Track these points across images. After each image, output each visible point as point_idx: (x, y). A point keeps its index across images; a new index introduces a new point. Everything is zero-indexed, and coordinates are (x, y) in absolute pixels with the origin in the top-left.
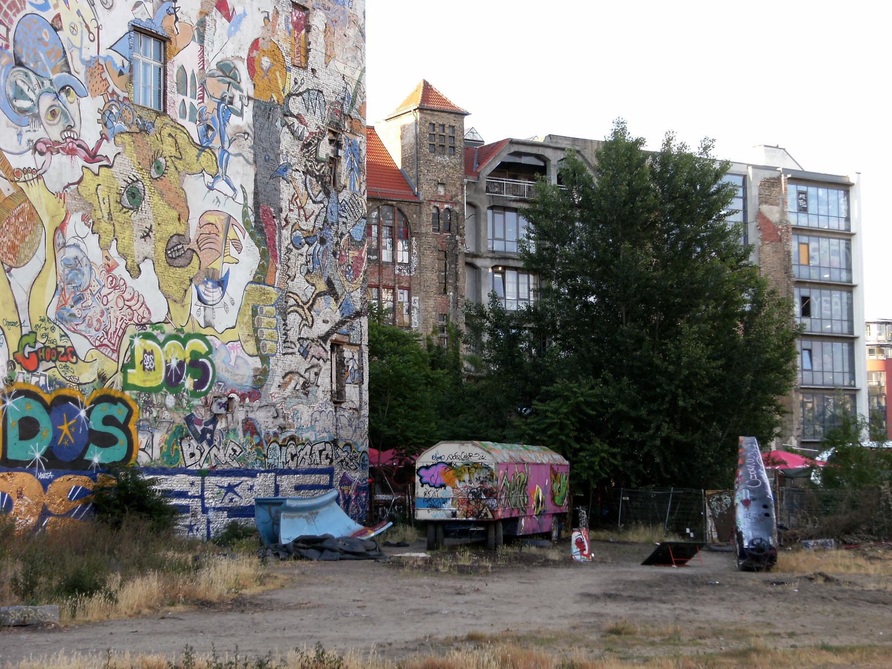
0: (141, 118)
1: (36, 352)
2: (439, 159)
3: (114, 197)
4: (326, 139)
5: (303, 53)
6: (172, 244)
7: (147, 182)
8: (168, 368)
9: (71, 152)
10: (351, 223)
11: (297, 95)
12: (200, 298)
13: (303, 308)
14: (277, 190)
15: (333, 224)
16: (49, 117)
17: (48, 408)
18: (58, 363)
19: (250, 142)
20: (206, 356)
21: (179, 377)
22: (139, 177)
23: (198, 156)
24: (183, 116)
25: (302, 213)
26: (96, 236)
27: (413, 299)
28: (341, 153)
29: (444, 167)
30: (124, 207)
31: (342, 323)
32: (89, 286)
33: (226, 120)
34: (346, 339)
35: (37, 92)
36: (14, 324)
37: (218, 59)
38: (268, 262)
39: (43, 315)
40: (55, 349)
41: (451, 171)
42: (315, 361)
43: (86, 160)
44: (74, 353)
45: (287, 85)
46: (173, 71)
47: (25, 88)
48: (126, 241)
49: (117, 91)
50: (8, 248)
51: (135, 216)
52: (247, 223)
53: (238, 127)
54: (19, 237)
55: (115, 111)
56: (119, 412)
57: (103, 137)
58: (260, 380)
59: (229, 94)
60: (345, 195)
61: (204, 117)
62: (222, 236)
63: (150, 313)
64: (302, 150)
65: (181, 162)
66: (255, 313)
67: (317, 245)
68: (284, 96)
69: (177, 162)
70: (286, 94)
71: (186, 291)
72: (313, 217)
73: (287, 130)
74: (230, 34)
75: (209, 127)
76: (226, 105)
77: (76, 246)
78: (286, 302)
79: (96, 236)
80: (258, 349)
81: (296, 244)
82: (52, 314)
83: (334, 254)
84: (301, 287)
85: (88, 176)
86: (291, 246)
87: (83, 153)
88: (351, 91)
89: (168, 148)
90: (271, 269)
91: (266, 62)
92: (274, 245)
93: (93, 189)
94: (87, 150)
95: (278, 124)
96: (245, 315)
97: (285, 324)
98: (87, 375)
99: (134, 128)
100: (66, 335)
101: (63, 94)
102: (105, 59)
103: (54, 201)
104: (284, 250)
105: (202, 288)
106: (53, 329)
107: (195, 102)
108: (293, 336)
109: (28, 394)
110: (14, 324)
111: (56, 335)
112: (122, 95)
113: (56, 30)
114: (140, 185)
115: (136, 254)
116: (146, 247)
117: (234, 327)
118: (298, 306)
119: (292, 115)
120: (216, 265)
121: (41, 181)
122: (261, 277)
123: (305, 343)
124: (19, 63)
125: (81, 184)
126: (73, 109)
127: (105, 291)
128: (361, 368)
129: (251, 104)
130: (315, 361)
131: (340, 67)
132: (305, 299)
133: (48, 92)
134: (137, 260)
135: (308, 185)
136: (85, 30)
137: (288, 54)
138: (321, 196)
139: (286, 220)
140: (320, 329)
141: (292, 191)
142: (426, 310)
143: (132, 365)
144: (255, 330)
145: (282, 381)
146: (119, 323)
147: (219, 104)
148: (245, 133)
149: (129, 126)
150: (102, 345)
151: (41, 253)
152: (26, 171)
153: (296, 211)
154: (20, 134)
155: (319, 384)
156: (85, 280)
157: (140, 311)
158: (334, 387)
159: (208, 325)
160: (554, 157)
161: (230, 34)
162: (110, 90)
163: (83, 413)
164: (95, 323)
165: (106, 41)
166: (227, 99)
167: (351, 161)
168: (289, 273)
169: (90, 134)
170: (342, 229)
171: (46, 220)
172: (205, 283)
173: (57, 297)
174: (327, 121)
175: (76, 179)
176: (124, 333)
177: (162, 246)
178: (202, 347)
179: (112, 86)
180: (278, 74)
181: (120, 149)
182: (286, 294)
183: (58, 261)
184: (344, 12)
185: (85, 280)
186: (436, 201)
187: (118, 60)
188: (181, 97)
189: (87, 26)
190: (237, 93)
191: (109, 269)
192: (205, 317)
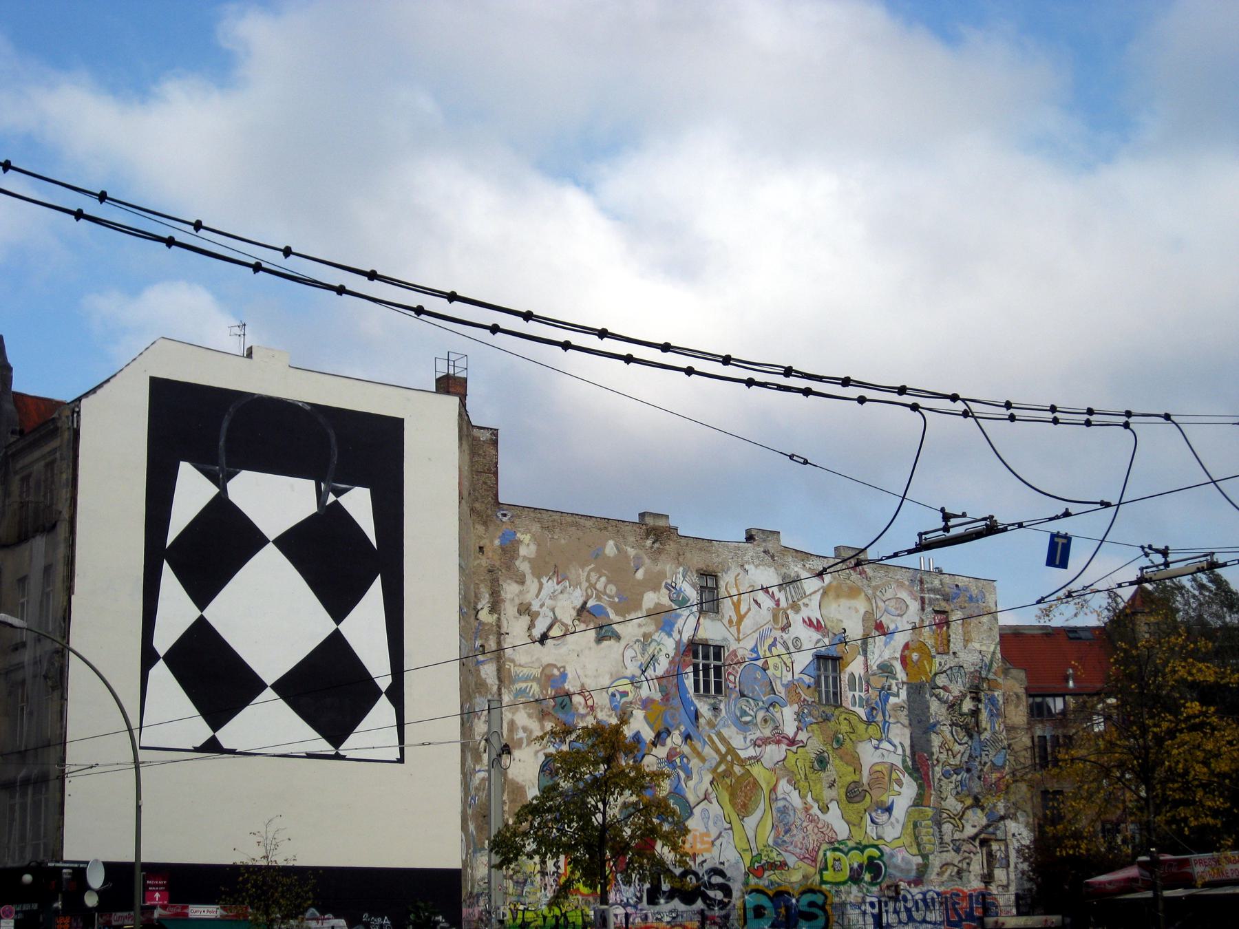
0: (824, 712)
1: (762, 866)
3: (808, 764)
4: (968, 698)
5: (945, 642)
6: (850, 788)
7: (831, 752)
8: (851, 869)
9: (778, 742)
10: (992, 753)
11: (942, 673)
12: (872, 821)
13: (954, 819)
14: (929, 741)
15: (977, 757)
16: (763, 723)
17: (771, 899)
18: (776, 871)
19: (905, 712)
20: (880, 858)
21: (859, 874)
22: (825, 749)
23: (867, 729)
24: (854, 704)
25: (950, 753)
26: (797, 791)
28: (980, 706)
30: (815, 770)
31: (988, 826)
33: (886, 700)
34: (993, 837)
35: (754, 710)
36: (747, 850)
37: (878, 662)
38: (924, 790)
39: (765, 843)
40: (774, 863)
42: (967, 855)
43: (788, 745)
44: (786, 864)
45: (933, 668)
46: (845, 677)
47: (747, 709)
48: (818, 791)
49: (807, 698)
50: (741, 806)
51: (823, 775)
52: (906, 768)
53: (896, 704)
54: (748, 798)
55: (806, 711)
56: (819, 899)
57: (799, 729)
58: (922, 871)
59: (888, 684)
60: (986, 735)
61: (870, 703)
62: (887, 778)
63: (836, 834)
64: (948, 710)
65: (854, 735)
66: (915, 826)
67: (964, 774)
68: (931, 676)
69: (851, 736)
70: (933, 674)
71: (862, 818)
72: (960, 755)
73: (935, 699)
74: (886, 644)
75: (873, 708)
76: (885, 693)
77: (784, 799)
78: (940, 816)
79: (797, 791)
80: (919, 850)
81: (946, 775)
82: (771, 842)
83: (979, 778)
84: (953, 804)
85: (790, 755)
86: (942, 778)
87: (786, 741)
88: (987, 661)
89: (845, 727)
90: (927, 795)
91: (915, 656)
92: (929, 779)
93: (793, 762)
94: (788, 739)
95: (927, 696)
96: (908, 829)
97: (941, 832)
98: (796, 877)
99: (820, 719)
100: (780, 854)
101: (771, 708)
102: (797, 680)
103: (768, 773)
104: (936, 780)
105: (874, 814)
106: (772, 851)
107: (862, 694)
108: (947, 838)
109: (758, 891)
110: (747, 850)
111: (774, 854)
112: (810, 700)
113: (765, 670)
114: (826, 754)
115: (825, 798)
116: (833, 793)
117: (899, 838)
118: (950, 817)
119: (939, 688)
120: (884, 798)
122: (919, 802)
123: (958, 843)
124: (743, 695)
125: (786, 760)
126: (778, 715)
127: (805, 824)
128: (1007, 857)
129: (905, 687)
130: (967, 855)
131: (977, 646)
132: (955, 812)
133: (761, 708)
134: (826, 802)
135: (954, 733)
136: (783, 665)
137: (933, 647)
138: (966, 739)
139: (937, 760)
140: (970, 831)
141: (941, 739)
143: (826, 868)
144: (916, 838)
145: (939, 870)
146: (815, 843)
148: (901, 707)
149: (817, 719)
150: (805, 858)
151: (762, 806)
152: (750, 758)
153: (945, 753)
154: (745, 738)
155: (971, 870)
156: (791, 819)
157: (830, 834)
158: (986, 871)
159: (880, 838)
161: (886, 644)
162: (802, 699)
163: (794, 901)
164: (799, 845)
167: (991, 710)
168: (942, 796)
169: (790, 729)
170: (985, 759)
171: (764, 786)
172: (876, 811)
173: (773, 831)
174: (968, 685)
175: (782, 758)
176: (819, 848)
177: (843, 791)
178: (876, 853)
179: (803, 696)
180: (925, 662)
181: (811, 734)
182: (939, 811)
183: (773, 809)
184: (978, 607)
185: (791, 819)
187: (807, 679)
188: (852, 693)
189: (785, 663)
190: (894, 682)
191: (807, 810)
192: (877, 833)
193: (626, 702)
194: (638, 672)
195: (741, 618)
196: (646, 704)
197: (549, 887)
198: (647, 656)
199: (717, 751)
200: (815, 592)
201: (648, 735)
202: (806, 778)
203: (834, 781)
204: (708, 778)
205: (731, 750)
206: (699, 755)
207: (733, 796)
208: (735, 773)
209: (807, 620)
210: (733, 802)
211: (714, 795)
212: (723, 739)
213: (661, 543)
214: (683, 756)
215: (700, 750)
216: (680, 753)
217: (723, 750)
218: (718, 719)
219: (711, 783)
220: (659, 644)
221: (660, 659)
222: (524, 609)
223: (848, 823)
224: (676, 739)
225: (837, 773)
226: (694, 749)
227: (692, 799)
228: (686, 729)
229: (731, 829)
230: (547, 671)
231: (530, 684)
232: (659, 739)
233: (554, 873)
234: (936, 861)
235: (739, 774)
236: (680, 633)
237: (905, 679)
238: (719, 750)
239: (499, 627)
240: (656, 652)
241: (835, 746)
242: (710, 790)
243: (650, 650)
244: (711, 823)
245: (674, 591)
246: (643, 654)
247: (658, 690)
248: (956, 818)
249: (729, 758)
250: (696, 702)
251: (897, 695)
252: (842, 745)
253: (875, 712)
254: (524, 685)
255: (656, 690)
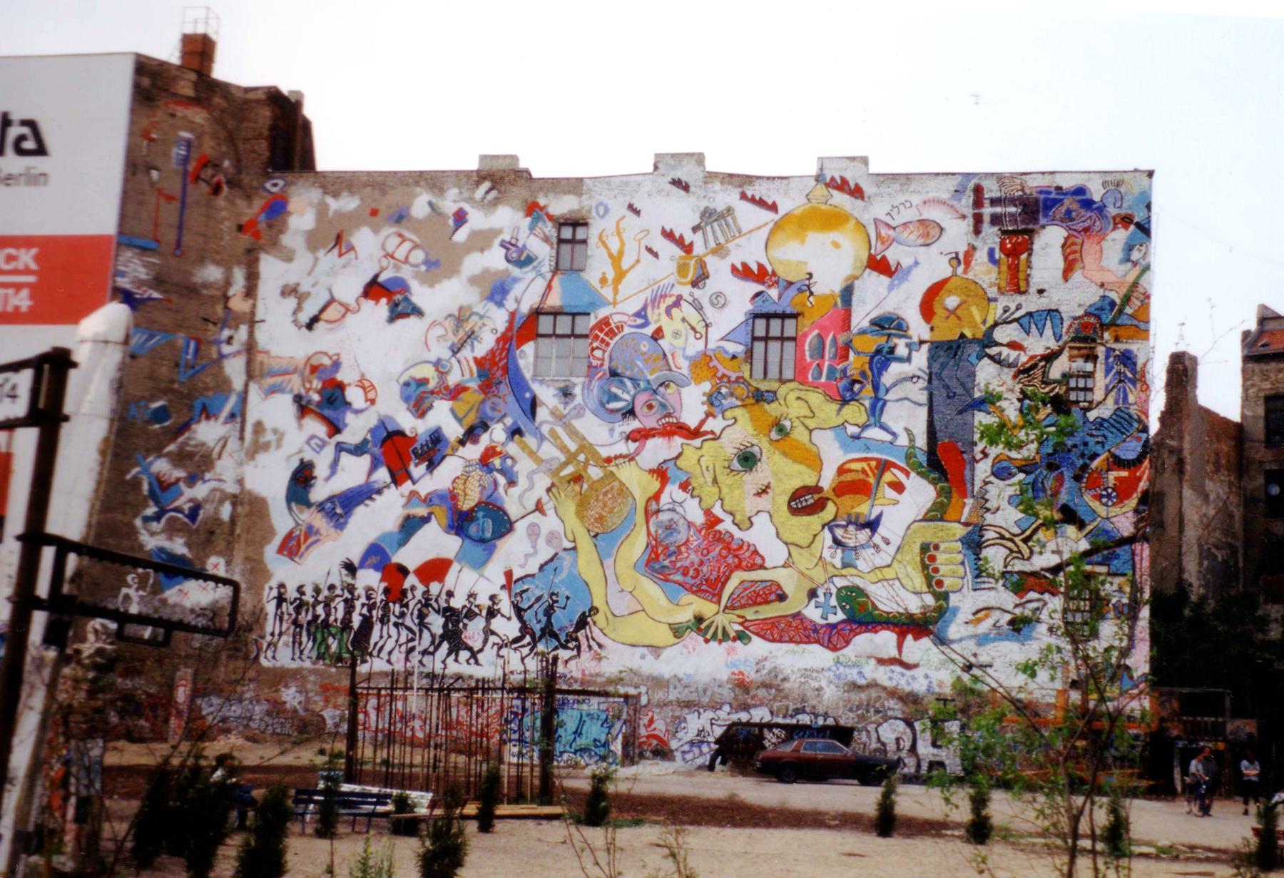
16: (645, 409)
19: (923, 383)
22: (755, 442)
26: (697, 500)
32: (688, 540)
35: (633, 392)
49: (729, 373)
51: (748, 477)
55: (724, 390)
57: (709, 415)
66: (925, 548)
68: (984, 328)
71: (815, 536)
74: (891, 288)
79: (697, 500)
93: (694, 461)
113: (656, 340)
114: (756, 450)
115: (747, 509)
116: (764, 502)
121: (633, 463)
122: (937, 513)
125: (682, 458)
126: (673, 401)
136: (692, 333)
147: (872, 358)
149: (742, 400)
154: (612, 430)
161: (891, 288)
165: (715, 334)
166: (886, 350)
168: (988, 505)
175: (675, 455)
183: (651, 523)
189: (693, 329)
193: (424, 392)
194: (446, 354)
195: (620, 275)
196: (455, 393)
197: (286, 617)
198: (461, 333)
199: (563, 449)
200: (759, 228)
201: (453, 431)
202: (715, 481)
203: (768, 487)
204: (543, 482)
205: (585, 447)
206: (532, 454)
207: (583, 505)
208: (590, 477)
209: (740, 267)
210: (580, 515)
211: (551, 505)
212: (573, 433)
213: (499, 192)
214: (506, 456)
215: (534, 447)
216: (500, 453)
217: (573, 447)
218: (569, 407)
219: (549, 490)
220: (482, 317)
221: (483, 335)
222: (289, 291)
223: (786, 543)
224: (497, 433)
225: (775, 474)
226: (525, 447)
227: (513, 510)
228: (515, 423)
229: (574, 548)
230: (314, 362)
231: (287, 377)
232: (471, 435)
233: (295, 599)
234: (965, 602)
235: (595, 478)
236: (518, 301)
237: (926, 335)
238: (565, 447)
239: (253, 313)
240: (476, 329)
241: (774, 435)
242: (545, 498)
243: (468, 327)
244: (541, 542)
245: (513, 249)
246: (455, 332)
247: (475, 374)
248: (1017, 539)
249: (582, 457)
250: (536, 387)
251: (908, 359)
252: (787, 434)
253: (857, 387)
254: (279, 379)
255: (471, 373)
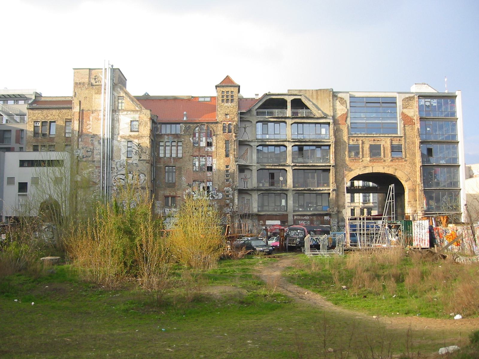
2: (226, 104)
27: (213, 160)
29: (228, 107)
41: (232, 109)
142: (219, 164)
160: (289, 99)
186: (224, 121)
